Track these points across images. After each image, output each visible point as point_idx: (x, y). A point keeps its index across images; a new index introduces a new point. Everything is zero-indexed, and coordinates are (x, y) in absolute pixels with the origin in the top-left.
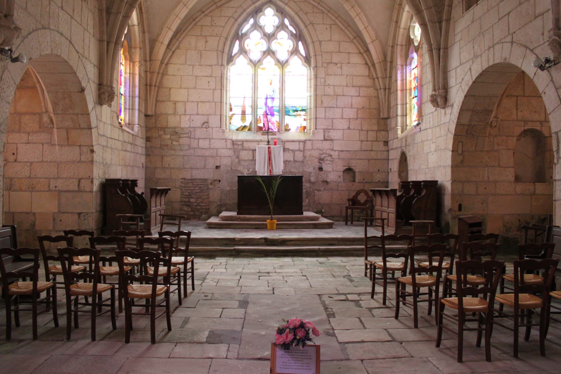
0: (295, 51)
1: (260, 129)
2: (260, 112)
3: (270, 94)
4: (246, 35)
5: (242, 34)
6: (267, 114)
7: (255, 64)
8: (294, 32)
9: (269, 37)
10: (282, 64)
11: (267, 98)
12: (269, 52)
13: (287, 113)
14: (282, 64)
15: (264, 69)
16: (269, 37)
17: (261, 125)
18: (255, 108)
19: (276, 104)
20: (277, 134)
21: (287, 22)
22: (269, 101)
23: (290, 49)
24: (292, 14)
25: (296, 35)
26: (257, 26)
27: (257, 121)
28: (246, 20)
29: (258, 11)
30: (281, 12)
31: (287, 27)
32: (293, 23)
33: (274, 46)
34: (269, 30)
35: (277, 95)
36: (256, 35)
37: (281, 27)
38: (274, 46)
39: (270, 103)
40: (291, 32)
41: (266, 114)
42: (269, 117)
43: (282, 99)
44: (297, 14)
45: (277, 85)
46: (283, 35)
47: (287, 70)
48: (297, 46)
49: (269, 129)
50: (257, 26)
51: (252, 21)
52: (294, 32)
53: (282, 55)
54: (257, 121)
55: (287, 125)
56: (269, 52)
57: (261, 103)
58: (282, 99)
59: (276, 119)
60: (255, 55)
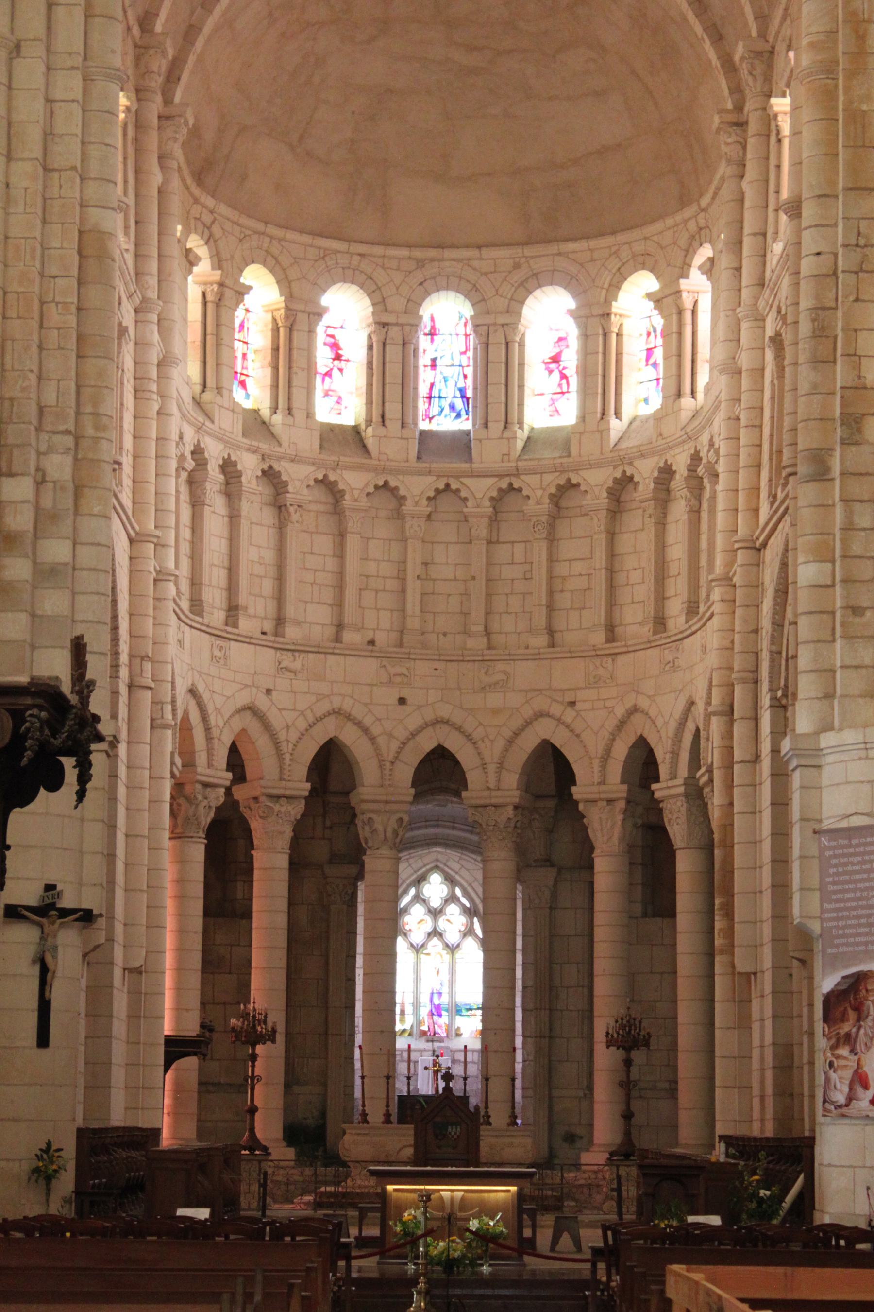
0: (469, 932)
1: (424, 1033)
2: (424, 1012)
3: (437, 987)
4: (405, 910)
5: (401, 909)
6: (433, 1014)
7: (418, 949)
8: (468, 905)
9: (435, 913)
10: (452, 949)
11: (432, 994)
12: (435, 933)
13: (458, 1012)
14: (452, 949)
15: (428, 954)
16: (435, 913)
17: (425, 1028)
18: (417, 1006)
19: (445, 1000)
20: (446, 1040)
21: (458, 891)
22: (436, 996)
23: (463, 928)
24: (465, 885)
25: (469, 909)
26: (418, 898)
27: (419, 1023)
28: (406, 892)
29: (421, 880)
30: (450, 880)
31: (458, 900)
32: (466, 893)
33: (442, 924)
34: (436, 903)
35: (445, 990)
36: (418, 911)
37: (451, 899)
38: (442, 924)
39: (436, 1001)
40: (463, 906)
41: (431, 1014)
42: (435, 1017)
43: (452, 994)
44: (470, 885)
45: (445, 976)
46: (453, 910)
47: (458, 955)
48: (472, 923)
49: (435, 1033)
50: (418, 898)
51: (413, 891)
52: (468, 905)
53: (452, 937)
54: (419, 1023)
55: (459, 1028)
56: (435, 933)
57: (425, 999)
58: (452, 994)
59: (444, 1020)
60: (417, 937)
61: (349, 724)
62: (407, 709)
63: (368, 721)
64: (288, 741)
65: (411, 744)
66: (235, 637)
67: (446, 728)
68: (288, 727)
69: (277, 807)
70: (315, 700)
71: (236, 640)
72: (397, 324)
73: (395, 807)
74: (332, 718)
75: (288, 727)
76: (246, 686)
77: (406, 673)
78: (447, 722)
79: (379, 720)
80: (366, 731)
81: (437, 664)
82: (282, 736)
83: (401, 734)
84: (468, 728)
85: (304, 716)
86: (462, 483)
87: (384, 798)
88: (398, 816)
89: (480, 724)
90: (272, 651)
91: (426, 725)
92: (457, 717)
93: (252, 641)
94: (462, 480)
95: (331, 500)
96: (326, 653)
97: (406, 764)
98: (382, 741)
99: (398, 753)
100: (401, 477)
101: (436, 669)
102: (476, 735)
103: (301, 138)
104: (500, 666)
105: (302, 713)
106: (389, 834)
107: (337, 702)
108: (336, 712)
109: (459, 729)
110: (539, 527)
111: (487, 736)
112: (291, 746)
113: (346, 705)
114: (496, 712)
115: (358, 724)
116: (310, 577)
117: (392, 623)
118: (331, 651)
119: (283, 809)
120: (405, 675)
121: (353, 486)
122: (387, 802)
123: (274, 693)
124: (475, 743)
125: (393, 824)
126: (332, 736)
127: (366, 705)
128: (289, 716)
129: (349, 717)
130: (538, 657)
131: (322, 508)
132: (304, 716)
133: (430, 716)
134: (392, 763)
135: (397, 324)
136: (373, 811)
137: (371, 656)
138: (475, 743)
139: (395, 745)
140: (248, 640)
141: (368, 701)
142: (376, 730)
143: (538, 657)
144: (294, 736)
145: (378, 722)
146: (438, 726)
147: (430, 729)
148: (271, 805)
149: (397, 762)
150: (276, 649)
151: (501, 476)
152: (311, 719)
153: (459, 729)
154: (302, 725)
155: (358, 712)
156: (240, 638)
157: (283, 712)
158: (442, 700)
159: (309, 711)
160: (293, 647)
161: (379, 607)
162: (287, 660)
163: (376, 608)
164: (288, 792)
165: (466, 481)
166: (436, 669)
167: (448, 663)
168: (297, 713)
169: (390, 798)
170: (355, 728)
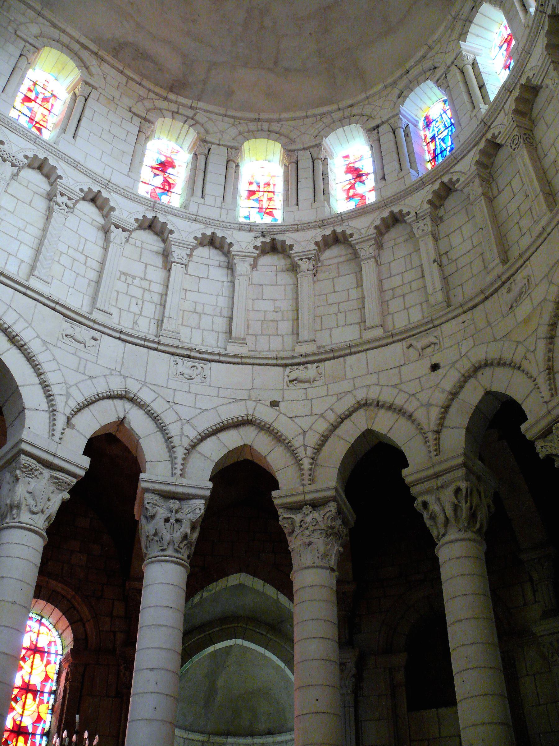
61: (382, 412)
62: (440, 372)
63: (399, 401)
64: (305, 446)
65: (455, 405)
66: (217, 358)
67: (488, 372)
68: (304, 433)
69: (298, 518)
70: (336, 400)
71: (219, 361)
72: (383, 123)
73: (447, 478)
74: (361, 412)
75: (304, 433)
76: (237, 400)
77: (435, 341)
78: (487, 364)
79: (414, 395)
80: (401, 411)
81: (463, 317)
82: (297, 443)
83: (440, 398)
84: (507, 356)
85: (324, 417)
86: (452, 173)
87: (431, 472)
88: (452, 488)
89: (518, 343)
90: (281, 369)
91: (465, 379)
92: (493, 353)
93: (244, 360)
94: (451, 171)
95: (350, 251)
96: (344, 356)
97: (455, 428)
98: (420, 415)
99: (443, 418)
100: (402, 203)
101: (463, 322)
102: (517, 359)
103: (275, 63)
104: (519, 277)
105: (321, 415)
106: (450, 512)
107: (361, 395)
108: (364, 405)
109: (501, 363)
110: (516, 142)
111: (528, 350)
112: (310, 451)
113: (373, 394)
114: (527, 321)
115: (390, 407)
116: (334, 309)
117: (423, 313)
118: (348, 351)
119: (308, 519)
120: (435, 344)
121: (360, 228)
122: (437, 476)
123: (281, 404)
124: (519, 368)
125: (448, 496)
126: (364, 428)
127: (395, 386)
128: (305, 423)
129: (379, 405)
130: (545, 235)
131: (342, 259)
132: (324, 417)
133: (466, 365)
134: (438, 432)
135: (383, 123)
136: (428, 492)
137: (394, 342)
138: (519, 368)
139: (435, 413)
140: (238, 360)
141: (398, 381)
142: (410, 407)
143: (545, 235)
144: (312, 439)
145: (412, 398)
146: (479, 374)
147: (472, 380)
148: (293, 516)
149: (444, 430)
150: (285, 366)
151: (477, 143)
152: (332, 417)
153: (501, 363)
154: (322, 427)
155: (387, 396)
156: (222, 359)
157: (296, 420)
158: (475, 345)
159: (330, 412)
160: (303, 360)
161: (407, 307)
162: (299, 373)
163: (405, 308)
164: (308, 497)
165: (456, 168)
166: (463, 322)
167: (474, 310)
168: (317, 417)
169: (438, 469)
170: (390, 413)
